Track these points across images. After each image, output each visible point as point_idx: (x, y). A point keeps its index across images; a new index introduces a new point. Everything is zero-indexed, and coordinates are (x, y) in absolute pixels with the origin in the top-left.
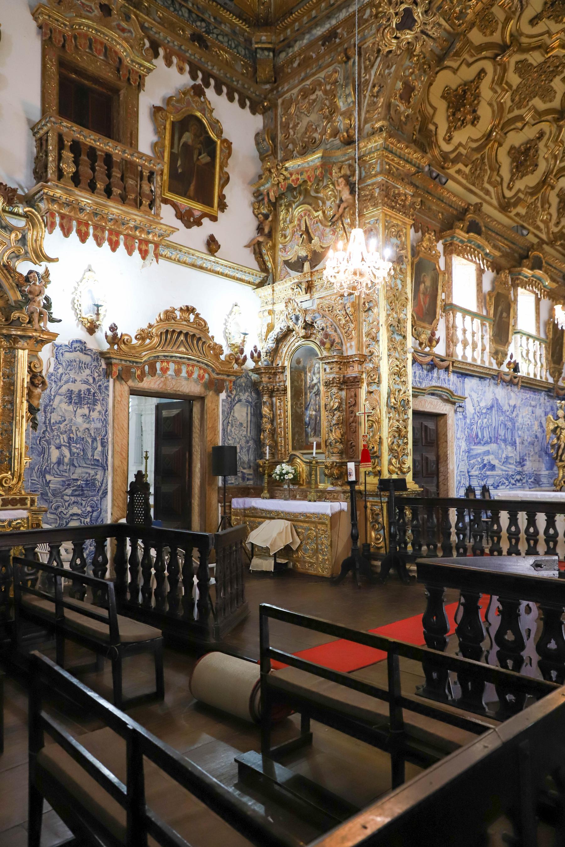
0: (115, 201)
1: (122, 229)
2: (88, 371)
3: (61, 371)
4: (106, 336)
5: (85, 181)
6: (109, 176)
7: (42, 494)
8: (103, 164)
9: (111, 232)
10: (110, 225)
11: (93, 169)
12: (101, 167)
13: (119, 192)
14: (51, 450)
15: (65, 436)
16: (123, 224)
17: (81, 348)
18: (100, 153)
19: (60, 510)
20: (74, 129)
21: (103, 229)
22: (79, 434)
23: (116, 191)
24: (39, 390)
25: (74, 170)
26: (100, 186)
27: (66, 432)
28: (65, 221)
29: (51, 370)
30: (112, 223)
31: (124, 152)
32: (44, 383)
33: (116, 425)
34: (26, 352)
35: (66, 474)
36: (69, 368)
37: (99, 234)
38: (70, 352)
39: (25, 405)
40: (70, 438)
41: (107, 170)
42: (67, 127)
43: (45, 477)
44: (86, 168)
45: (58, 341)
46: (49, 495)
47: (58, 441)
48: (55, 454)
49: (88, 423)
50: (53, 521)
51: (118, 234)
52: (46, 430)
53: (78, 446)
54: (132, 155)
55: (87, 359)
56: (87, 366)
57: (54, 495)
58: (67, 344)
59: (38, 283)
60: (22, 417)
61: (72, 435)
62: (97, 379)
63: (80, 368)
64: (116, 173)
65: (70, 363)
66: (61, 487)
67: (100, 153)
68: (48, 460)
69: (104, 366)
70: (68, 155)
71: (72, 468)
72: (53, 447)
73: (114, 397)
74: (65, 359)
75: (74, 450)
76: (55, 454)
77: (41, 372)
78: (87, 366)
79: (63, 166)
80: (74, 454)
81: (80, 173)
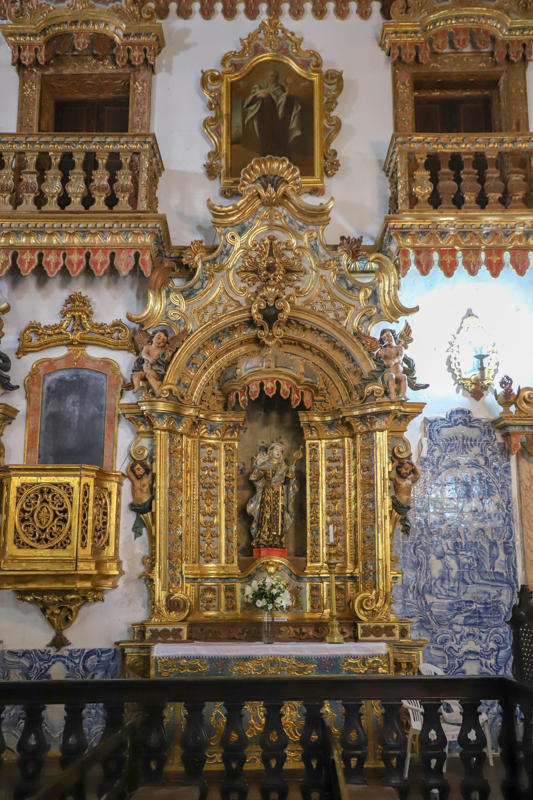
0: (493, 209)
1: (505, 242)
2: (476, 450)
3: (437, 454)
4: (497, 397)
5: (447, 198)
6: (482, 180)
7: (421, 621)
8: (471, 169)
9: (489, 251)
10: (485, 243)
11: (458, 180)
12: (468, 173)
13: (499, 195)
14: (430, 561)
15: (449, 541)
16: (507, 236)
17: (465, 421)
18: (467, 157)
19: (448, 645)
20: (429, 139)
21: (477, 251)
22: (469, 538)
23: (494, 196)
24: (408, 482)
25: (431, 189)
26: (469, 197)
27: (450, 535)
28: (422, 256)
29: (424, 454)
30: (490, 238)
31: (502, 142)
32: (414, 471)
33: (525, 523)
34: (386, 433)
35: (454, 594)
36: (449, 448)
37: (473, 260)
38: (449, 427)
39: (388, 502)
40: (456, 544)
41: (477, 174)
42: (419, 142)
43: (424, 599)
44: (448, 182)
45: (427, 413)
46: (433, 623)
47: (439, 549)
48: (437, 567)
49: (482, 521)
50: (439, 659)
51: (500, 251)
52: (422, 534)
53: (469, 554)
54: (514, 142)
55: (474, 433)
56: (473, 442)
57: (438, 623)
58: (444, 416)
59: (394, 344)
60: (385, 518)
61: (458, 540)
62: (490, 459)
63: (464, 446)
64: (492, 173)
65: (449, 441)
66: (448, 612)
67: (467, 157)
68: (427, 575)
69: (500, 440)
70: (423, 174)
71: (462, 585)
72: (433, 557)
73: (520, 481)
74: (442, 437)
75: (464, 560)
76: (437, 567)
77: (409, 458)
78: (473, 442)
79: (417, 190)
80: (464, 565)
81: (440, 190)
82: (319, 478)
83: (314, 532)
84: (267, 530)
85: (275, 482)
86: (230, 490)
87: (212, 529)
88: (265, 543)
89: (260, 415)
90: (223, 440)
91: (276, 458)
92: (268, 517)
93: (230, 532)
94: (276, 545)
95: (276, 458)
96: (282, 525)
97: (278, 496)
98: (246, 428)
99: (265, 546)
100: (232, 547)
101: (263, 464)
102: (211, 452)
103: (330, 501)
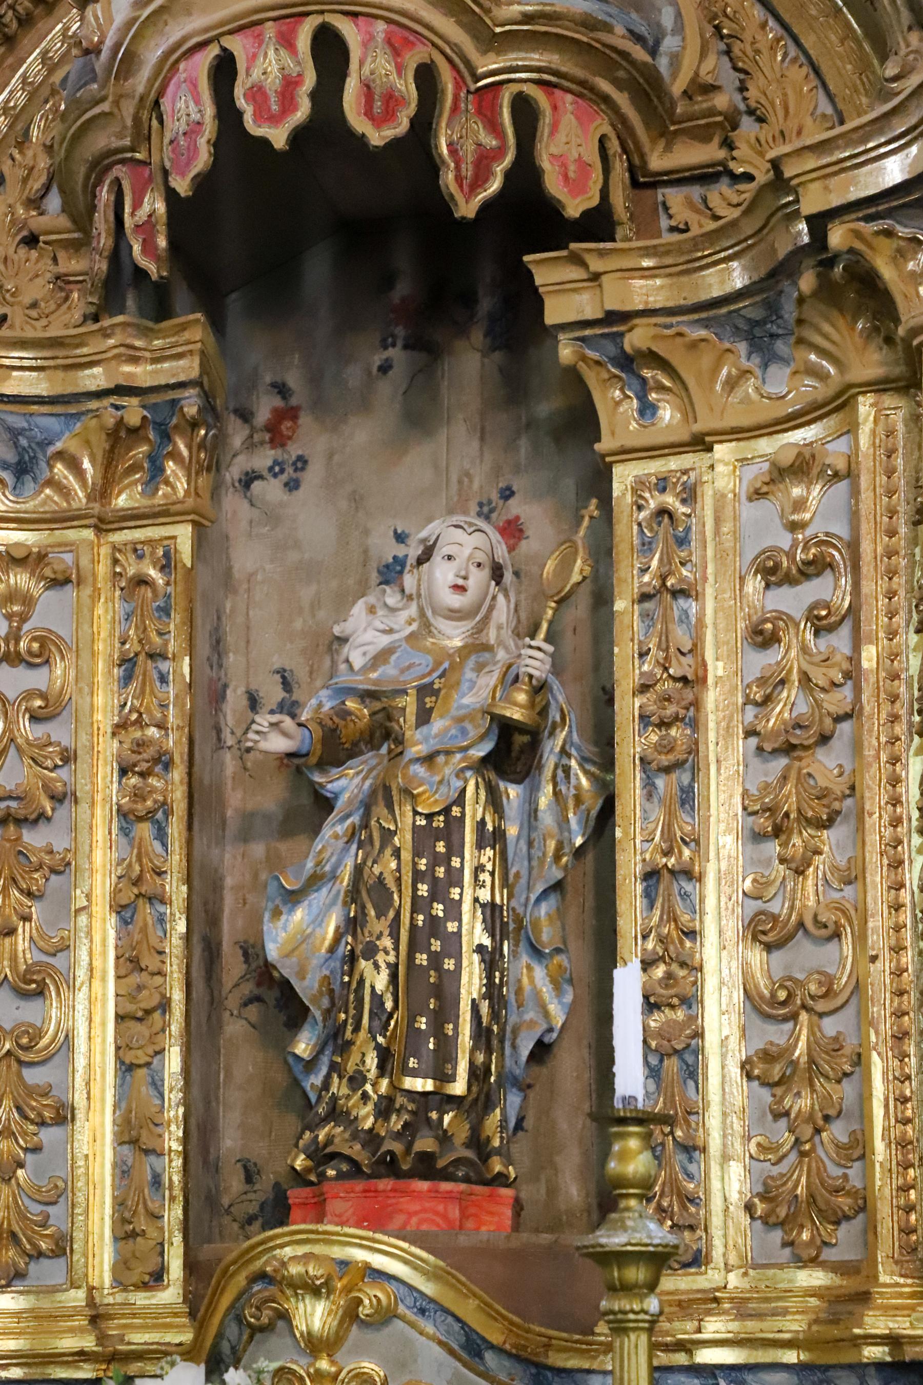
82: (696, 704)
83: (672, 1065)
84: (372, 1061)
85: (429, 759)
86: (145, 830)
87: (32, 1076)
88: (356, 1150)
89: (385, 369)
90: (103, 525)
91: (455, 615)
92: (381, 982)
93: (146, 1091)
94: (426, 1158)
95: (455, 615)
96: (481, 1035)
97: (455, 849)
98: (301, 463)
99: (356, 1169)
100: (157, 1181)
101: (381, 657)
102: (28, 601)
103: (773, 848)
